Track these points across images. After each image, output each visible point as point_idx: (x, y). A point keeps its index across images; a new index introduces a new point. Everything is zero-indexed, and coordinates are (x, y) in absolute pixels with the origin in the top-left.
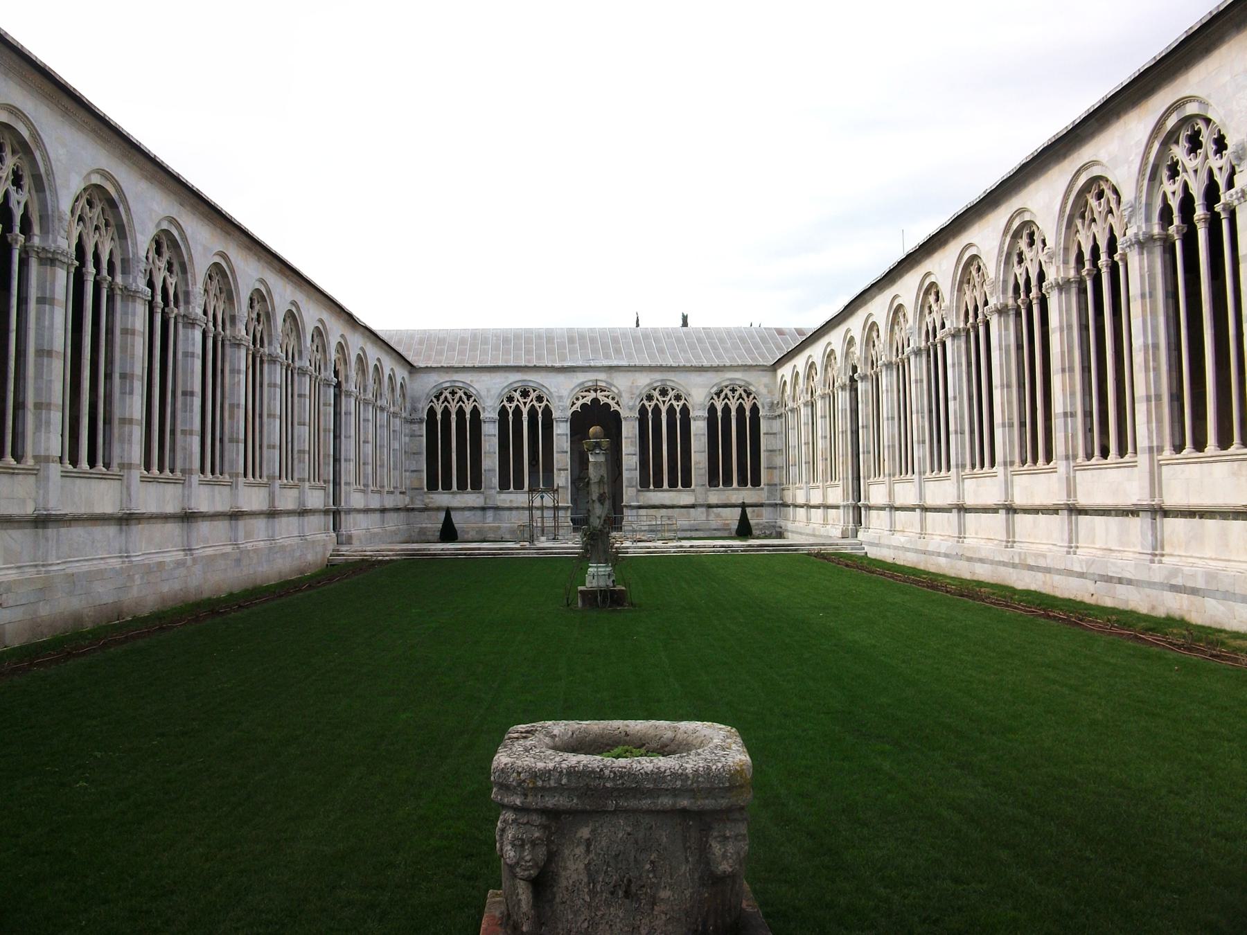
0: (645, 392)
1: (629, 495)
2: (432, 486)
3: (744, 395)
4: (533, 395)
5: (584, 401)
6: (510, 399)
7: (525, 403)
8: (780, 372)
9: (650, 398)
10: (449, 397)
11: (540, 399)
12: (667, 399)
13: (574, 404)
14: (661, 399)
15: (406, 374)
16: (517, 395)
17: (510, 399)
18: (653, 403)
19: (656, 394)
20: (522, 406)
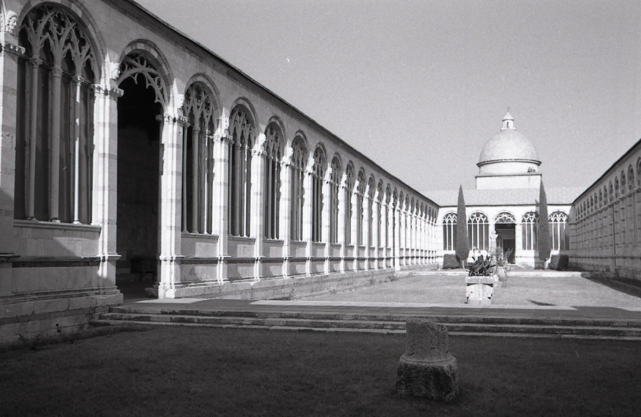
0: (524, 213)
1: (517, 253)
2: (445, 248)
3: (563, 215)
4: (481, 216)
5: (501, 218)
6: (472, 217)
7: (478, 219)
8: (576, 207)
9: (526, 216)
10: (451, 216)
11: (483, 217)
12: (533, 216)
13: (496, 219)
14: (530, 217)
15: (435, 209)
16: (475, 216)
17: (472, 217)
18: (527, 218)
19: (529, 215)
20: (477, 220)
